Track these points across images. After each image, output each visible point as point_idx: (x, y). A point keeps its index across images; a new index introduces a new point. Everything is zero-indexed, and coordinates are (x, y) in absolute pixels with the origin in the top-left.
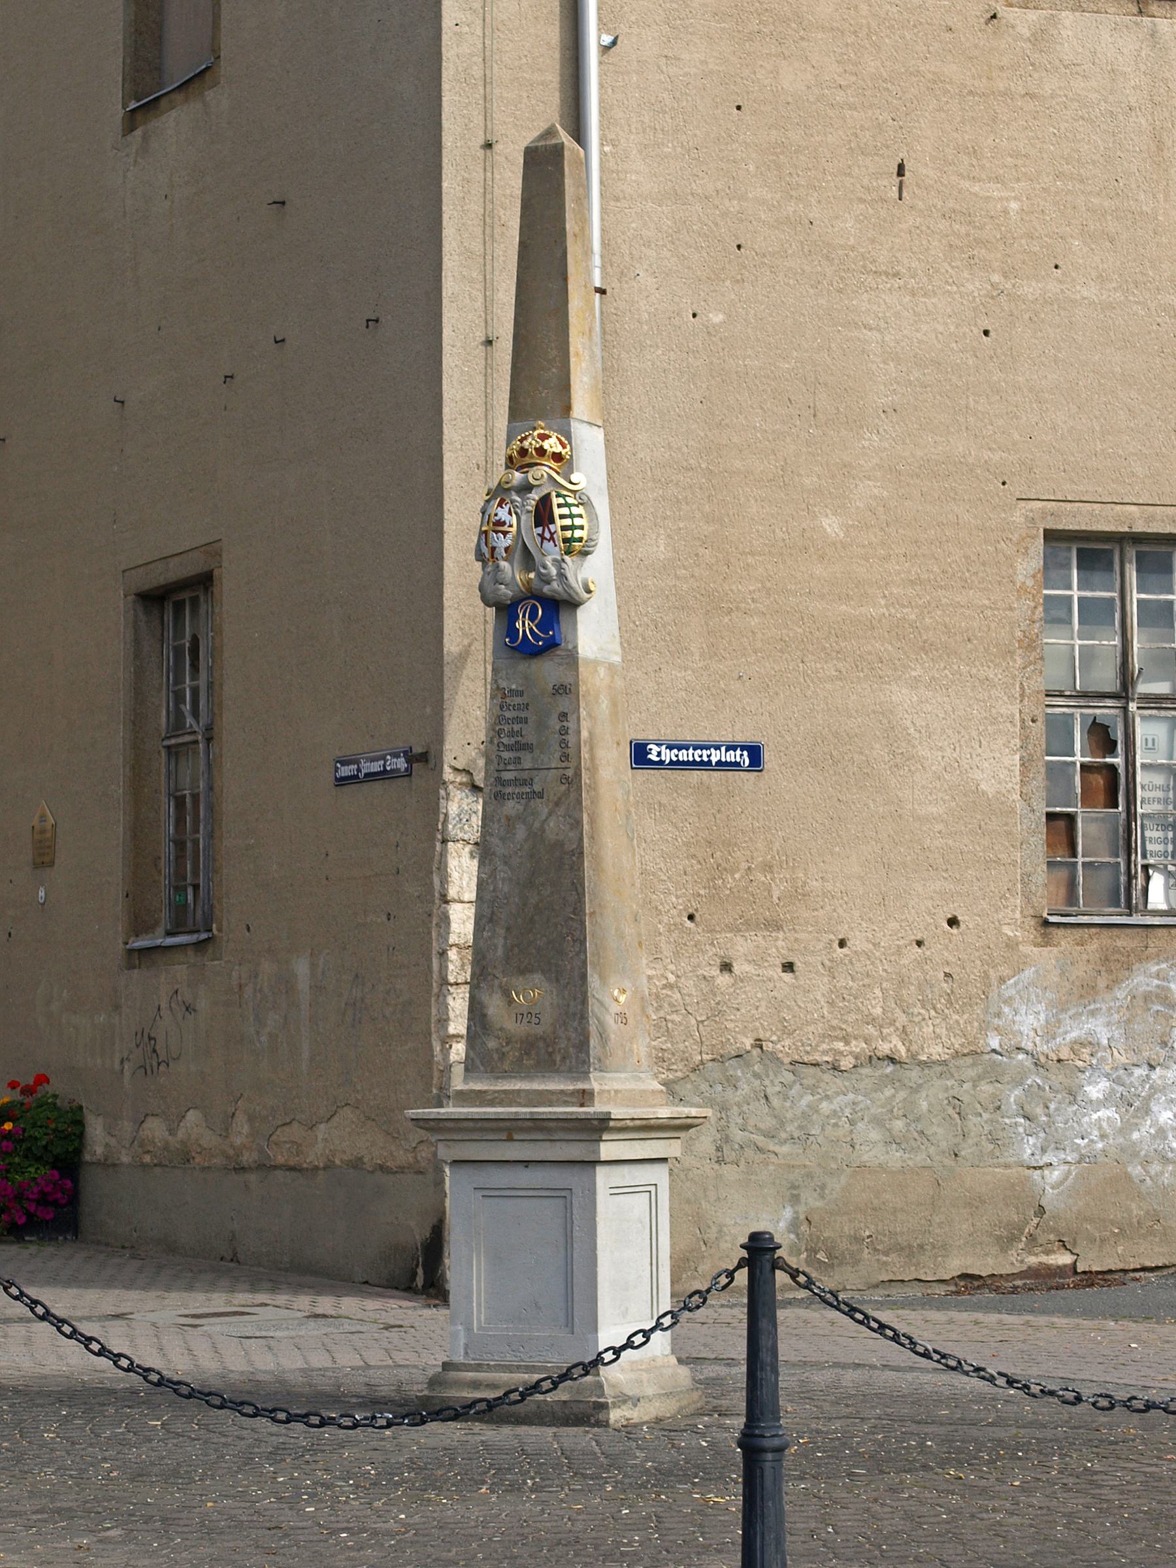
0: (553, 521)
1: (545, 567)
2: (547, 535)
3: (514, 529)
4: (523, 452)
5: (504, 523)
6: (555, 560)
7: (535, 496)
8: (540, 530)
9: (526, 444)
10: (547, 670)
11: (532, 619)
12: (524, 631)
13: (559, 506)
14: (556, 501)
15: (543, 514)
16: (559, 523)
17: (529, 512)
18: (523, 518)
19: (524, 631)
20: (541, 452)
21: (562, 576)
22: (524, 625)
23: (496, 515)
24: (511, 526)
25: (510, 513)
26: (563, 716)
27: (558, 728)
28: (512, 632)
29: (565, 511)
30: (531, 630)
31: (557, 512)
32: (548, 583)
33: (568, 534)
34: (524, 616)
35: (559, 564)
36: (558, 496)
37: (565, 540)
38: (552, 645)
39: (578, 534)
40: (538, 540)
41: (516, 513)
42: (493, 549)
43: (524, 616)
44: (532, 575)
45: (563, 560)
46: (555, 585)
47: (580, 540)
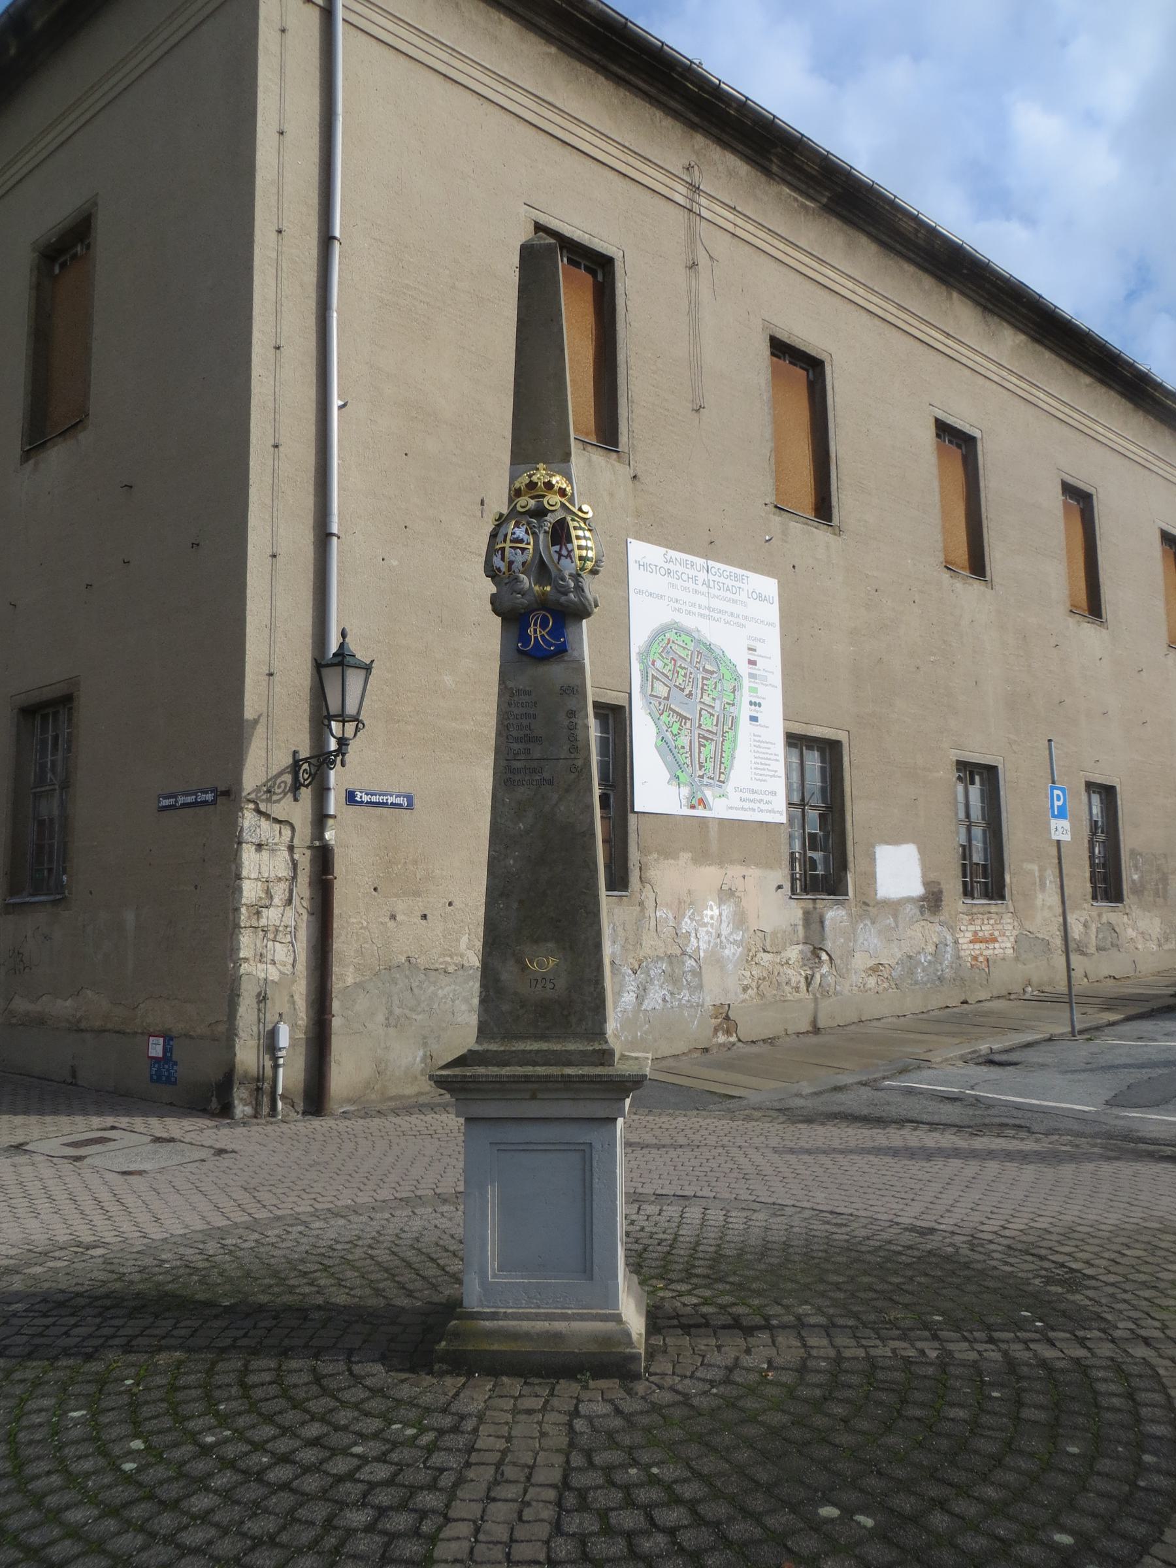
0: (570, 541)
1: (563, 579)
2: (564, 552)
3: (530, 547)
4: (532, 485)
5: (521, 541)
6: (570, 575)
7: (551, 519)
8: (557, 548)
9: (534, 479)
10: (556, 672)
11: (543, 626)
12: (536, 638)
13: (575, 528)
14: (572, 524)
15: (561, 534)
16: (576, 542)
17: (546, 532)
18: (541, 536)
19: (536, 638)
20: (549, 486)
21: (579, 589)
22: (535, 632)
23: (513, 533)
24: (528, 544)
25: (527, 532)
26: (571, 714)
27: (566, 723)
28: (525, 638)
29: (580, 533)
30: (542, 636)
31: (574, 533)
32: (566, 594)
33: (584, 553)
34: (535, 624)
35: (576, 577)
36: (573, 520)
37: (581, 558)
38: (562, 650)
39: (591, 554)
40: (556, 557)
41: (534, 533)
42: (511, 563)
43: (535, 624)
44: (548, 588)
45: (579, 575)
46: (572, 595)
47: (590, 559)
